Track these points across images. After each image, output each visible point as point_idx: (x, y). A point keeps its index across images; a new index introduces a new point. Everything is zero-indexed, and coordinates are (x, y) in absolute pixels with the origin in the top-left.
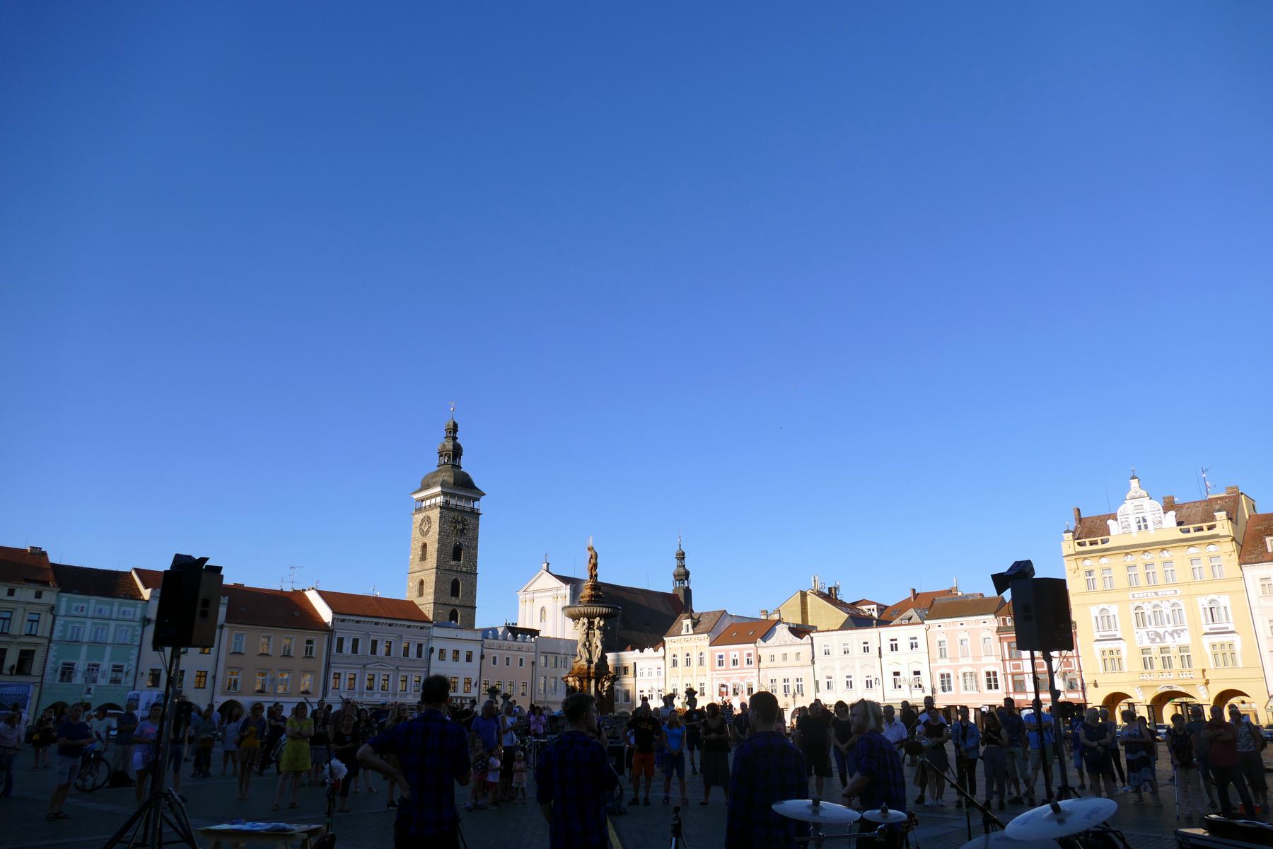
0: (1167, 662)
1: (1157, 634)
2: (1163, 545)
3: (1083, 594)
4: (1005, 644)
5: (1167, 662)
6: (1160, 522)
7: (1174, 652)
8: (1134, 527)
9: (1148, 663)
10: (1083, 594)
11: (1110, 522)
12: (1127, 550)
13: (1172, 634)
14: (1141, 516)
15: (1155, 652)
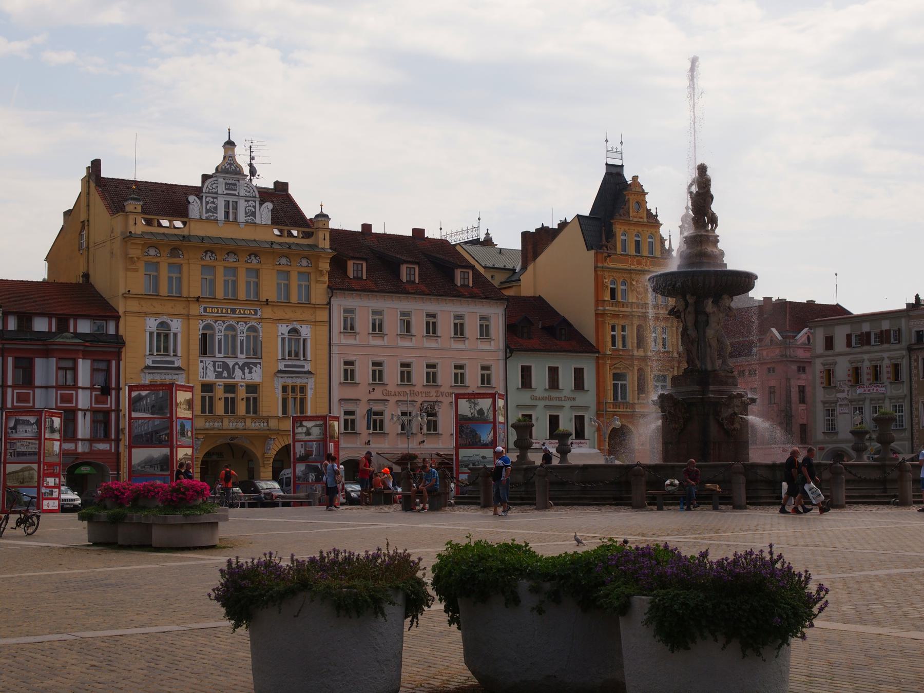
0: (230, 405)
1: (225, 366)
2: (254, 251)
3: (139, 297)
4: (10, 360)
5: (230, 405)
6: (254, 214)
7: (242, 393)
8: (221, 216)
9: (208, 406)
10: (139, 297)
11: (191, 198)
12: (211, 247)
13: (242, 368)
14: (231, 199)
15: (220, 392)
